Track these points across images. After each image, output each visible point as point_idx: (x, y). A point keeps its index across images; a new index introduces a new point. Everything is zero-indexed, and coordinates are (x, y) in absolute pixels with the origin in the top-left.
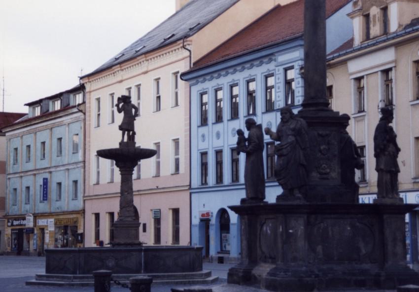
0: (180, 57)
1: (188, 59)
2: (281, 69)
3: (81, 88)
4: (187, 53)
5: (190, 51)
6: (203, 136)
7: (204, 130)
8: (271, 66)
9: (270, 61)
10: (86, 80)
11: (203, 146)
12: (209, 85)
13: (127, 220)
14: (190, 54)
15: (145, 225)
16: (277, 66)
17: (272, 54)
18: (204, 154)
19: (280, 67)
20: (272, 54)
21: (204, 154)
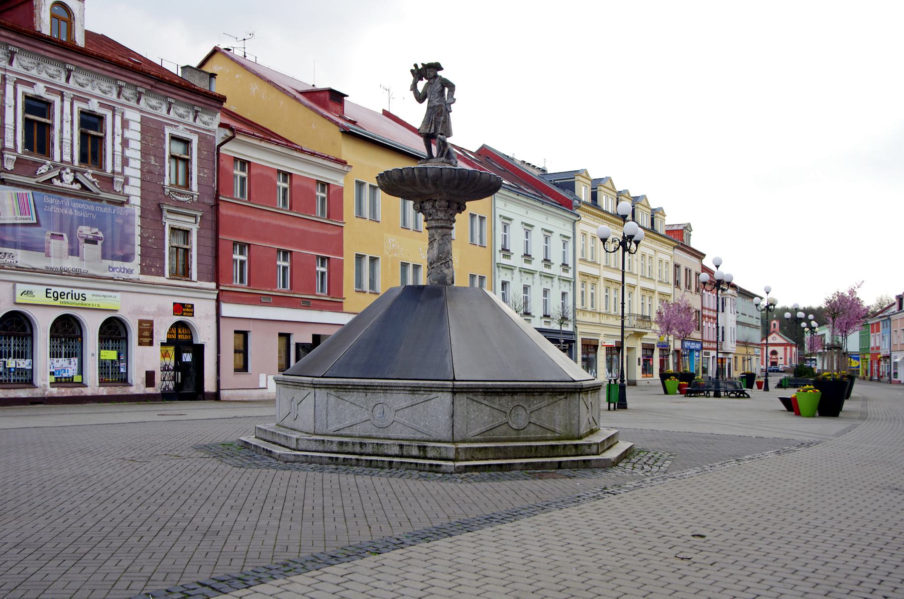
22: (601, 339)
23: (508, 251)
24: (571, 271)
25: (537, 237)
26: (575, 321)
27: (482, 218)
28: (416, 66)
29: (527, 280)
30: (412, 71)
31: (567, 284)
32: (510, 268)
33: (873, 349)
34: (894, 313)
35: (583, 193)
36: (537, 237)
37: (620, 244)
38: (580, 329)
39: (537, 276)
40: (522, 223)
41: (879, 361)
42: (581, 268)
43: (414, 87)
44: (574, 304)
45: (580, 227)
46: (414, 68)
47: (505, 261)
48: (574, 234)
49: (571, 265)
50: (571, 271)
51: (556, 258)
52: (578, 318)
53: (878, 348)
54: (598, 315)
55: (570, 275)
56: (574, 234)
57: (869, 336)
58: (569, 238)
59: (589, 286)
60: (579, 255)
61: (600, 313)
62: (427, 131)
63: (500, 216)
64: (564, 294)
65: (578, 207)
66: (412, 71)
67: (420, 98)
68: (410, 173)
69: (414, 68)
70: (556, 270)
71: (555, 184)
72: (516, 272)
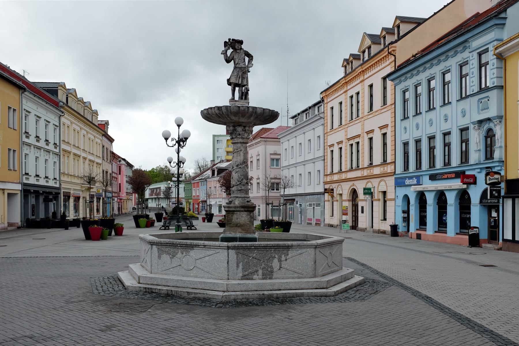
0: (388, 62)
1: (394, 62)
2: (475, 54)
3: (322, 100)
4: (393, 58)
5: (395, 56)
6: (405, 128)
7: (406, 123)
8: (466, 55)
9: (465, 48)
10: (324, 94)
11: (405, 137)
12: (410, 83)
13: (349, 200)
14: (395, 58)
15: (362, 208)
16: (470, 52)
17: (466, 41)
18: (406, 144)
19: (474, 53)
20: (466, 41)
21: (406, 144)
22: (72, 192)
23: (28, 133)
24: (58, 148)
25: (42, 123)
26: (60, 180)
27: (14, 110)
28: (229, 40)
29: (38, 153)
30: (225, 42)
31: (56, 156)
32: (29, 145)
33: (194, 196)
34: (208, 178)
35: (61, 97)
36: (42, 123)
37: (177, 142)
38: (63, 186)
39: (42, 150)
40: (35, 115)
41: (198, 204)
42: (63, 146)
43: (225, 53)
44: (60, 170)
45: (63, 119)
46: (228, 41)
47: (26, 140)
48: (60, 124)
49: (58, 144)
50: (58, 148)
51: (51, 141)
52: (62, 179)
53: (198, 196)
54: (70, 177)
55: (57, 151)
56: (60, 124)
57: (191, 189)
58: (57, 126)
59: (66, 158)
60: (62, 139)
61: (71, 175)
62: (237, 82)
63: (25, 109)
64: (55, 162)
65: (62, 107)
66: (225, 42)
67: (228, 61)
68: (247, 109)
69: (228, 41)
70: (51, 147)
71: (45, 90)
72: (32, 147)
